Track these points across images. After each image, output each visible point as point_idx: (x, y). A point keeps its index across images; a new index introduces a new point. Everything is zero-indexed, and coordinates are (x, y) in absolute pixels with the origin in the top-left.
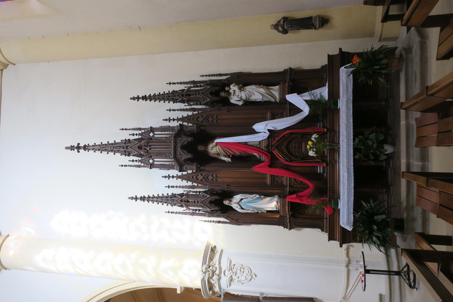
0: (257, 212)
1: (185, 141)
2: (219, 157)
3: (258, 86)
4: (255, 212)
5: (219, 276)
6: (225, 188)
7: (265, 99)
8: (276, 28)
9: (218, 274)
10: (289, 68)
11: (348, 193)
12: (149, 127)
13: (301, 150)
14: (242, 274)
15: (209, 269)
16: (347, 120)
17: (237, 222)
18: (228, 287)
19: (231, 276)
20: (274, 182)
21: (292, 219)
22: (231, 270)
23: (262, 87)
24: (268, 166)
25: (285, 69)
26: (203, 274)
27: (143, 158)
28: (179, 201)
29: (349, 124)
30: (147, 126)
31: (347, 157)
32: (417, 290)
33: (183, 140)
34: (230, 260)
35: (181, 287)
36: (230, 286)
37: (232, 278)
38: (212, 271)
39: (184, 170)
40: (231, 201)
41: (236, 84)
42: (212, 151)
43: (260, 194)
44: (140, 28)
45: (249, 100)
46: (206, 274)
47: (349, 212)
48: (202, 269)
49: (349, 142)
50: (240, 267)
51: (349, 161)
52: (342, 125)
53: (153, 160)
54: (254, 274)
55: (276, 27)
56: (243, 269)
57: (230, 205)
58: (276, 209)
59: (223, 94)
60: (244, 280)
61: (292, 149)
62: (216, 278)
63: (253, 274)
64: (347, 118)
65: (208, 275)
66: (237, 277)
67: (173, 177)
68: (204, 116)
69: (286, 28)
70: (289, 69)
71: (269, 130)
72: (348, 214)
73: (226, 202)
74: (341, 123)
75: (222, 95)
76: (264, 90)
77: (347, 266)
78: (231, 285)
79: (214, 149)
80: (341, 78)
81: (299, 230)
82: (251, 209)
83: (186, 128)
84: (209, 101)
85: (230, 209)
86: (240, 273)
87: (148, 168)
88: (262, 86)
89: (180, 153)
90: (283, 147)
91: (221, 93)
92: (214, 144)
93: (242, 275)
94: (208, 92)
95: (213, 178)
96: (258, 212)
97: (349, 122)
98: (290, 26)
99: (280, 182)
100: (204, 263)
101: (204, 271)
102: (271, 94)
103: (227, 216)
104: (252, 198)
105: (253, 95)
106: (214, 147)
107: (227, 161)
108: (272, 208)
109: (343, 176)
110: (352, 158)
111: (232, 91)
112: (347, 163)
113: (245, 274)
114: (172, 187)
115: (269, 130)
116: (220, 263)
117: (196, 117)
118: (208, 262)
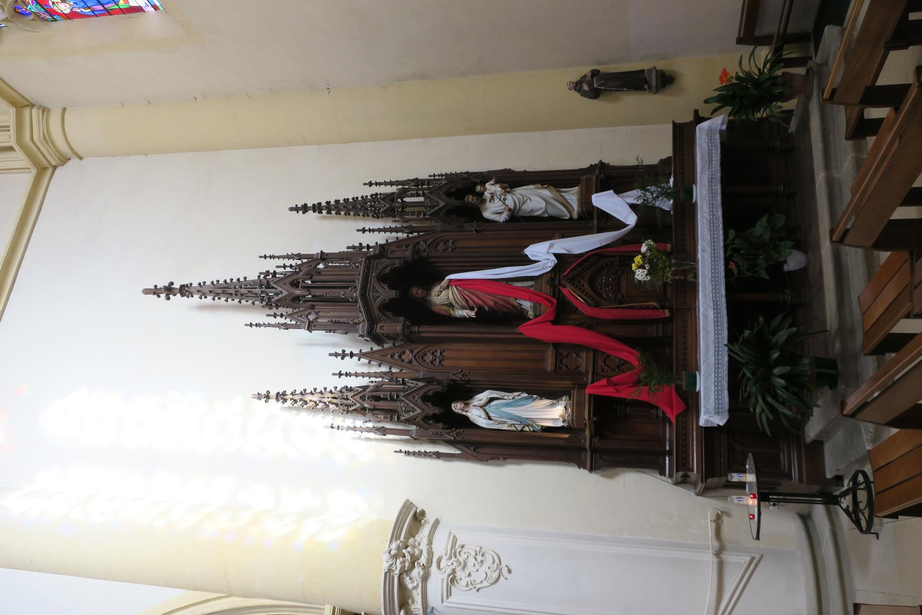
0: (522, 430)
1: (388, 267)
2: (452, 312)
3: (539, 186)
4: (516, 428)
5: (426, 568)
6: (458, 375)
7: (552, 212)
8: (578, 88)
9: (425, 564)
10: (599, 162)
11: (717, 349)
12: (319, 252)
14: (477, 566)
15: (404, 551)
16: (711, 213)
17: (478, 452)
18: (442, 602)
19: (454, 571)
20: (561, 368)
21: (596, 440)
22: (455, 556)
23: (546, 188)
25: (591, 165)
26: (391, 558)
27: (297, 309)
28: (358, 399)
29: (715, 221)
30: (314, 250)
31: (713, 279)
32: (878, 538)
33: (379, 297)
34: (455, 536)
35: (334, 608)
36: (448, 598)
37: (455, 577)
38: (410, 555)
39: (389, 255)
40: (467, 405)
41: (497, 182)
42: (439, 297)
43: (530, 392)
44: (328, 89)
45: (521, 214)
46: (396, 560)
47: (720, 388)
48: (389, 547)
49: (716, 252)
50: (476, 552)
51: (717, 287)
52: (701, 221)
53: (317, 313)
54: (507, 566)
55: (577, 86)
56: (483, 555)
57: (464, 413)
58: (563, 422)
59: (470, 198)
60: (482, 582)
61: (601, 286)
62: (419, 573)
63: (503, 565)
64: (711, 210)
65: (401, 563)
66: (467, 574)
67: (352, 355)
68: (428, 242)
69: (595, 86)
70: (600, 166)
71: (556, 255)
72: (716, 393)
73: (456, 405)
74: (699, 217)
75: (468, 199)
76: (550, 192)
77: (718, 553)
78: (451, 595)
79: (441, 296)
80: (699, 142)
81: (611, 477)
82: (510, 422)
83: (392, 252)
84: (443, 207)
85: (465, 422)
86: (474, 565)
87: (304, 328)
88: (546, 186)
89: (373, 288)
90: (582, 280)
91: (467, 197)
92: (444, 283)
93: (478, 570)
94: (441, 191)
95: (435, 360)
96: (524, 429)
97: (715, 217)
98: (603, 81)
99: (574, 367)
100: (395, 535)
101: (393, 553)
102: (562, 200)
103: (456, 434)
104: (513, 399)
105: (529, 201)
106: (444, 290)
107: (468, 315)
108: (555, 420)
109: (706, 317)
110: (722, 282)
111: (488, 193)
112: (714, 291)
113: (485, 567)
114: (347, 375)
115: (556, 255)
116: (430, 543)
117: (412, 243)
118: (405, 538)
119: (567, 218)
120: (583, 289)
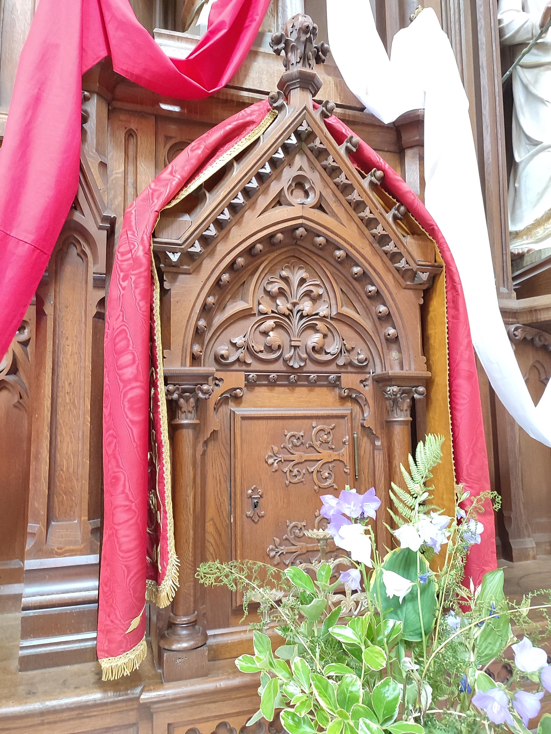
13: (272, 384)
24: (103, 53)
61: (281, 292)
119: (512, 228)
120: (263, 201)
